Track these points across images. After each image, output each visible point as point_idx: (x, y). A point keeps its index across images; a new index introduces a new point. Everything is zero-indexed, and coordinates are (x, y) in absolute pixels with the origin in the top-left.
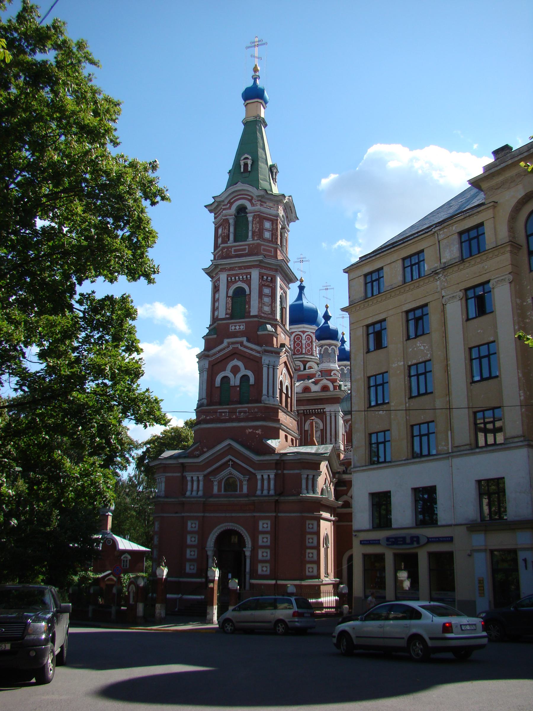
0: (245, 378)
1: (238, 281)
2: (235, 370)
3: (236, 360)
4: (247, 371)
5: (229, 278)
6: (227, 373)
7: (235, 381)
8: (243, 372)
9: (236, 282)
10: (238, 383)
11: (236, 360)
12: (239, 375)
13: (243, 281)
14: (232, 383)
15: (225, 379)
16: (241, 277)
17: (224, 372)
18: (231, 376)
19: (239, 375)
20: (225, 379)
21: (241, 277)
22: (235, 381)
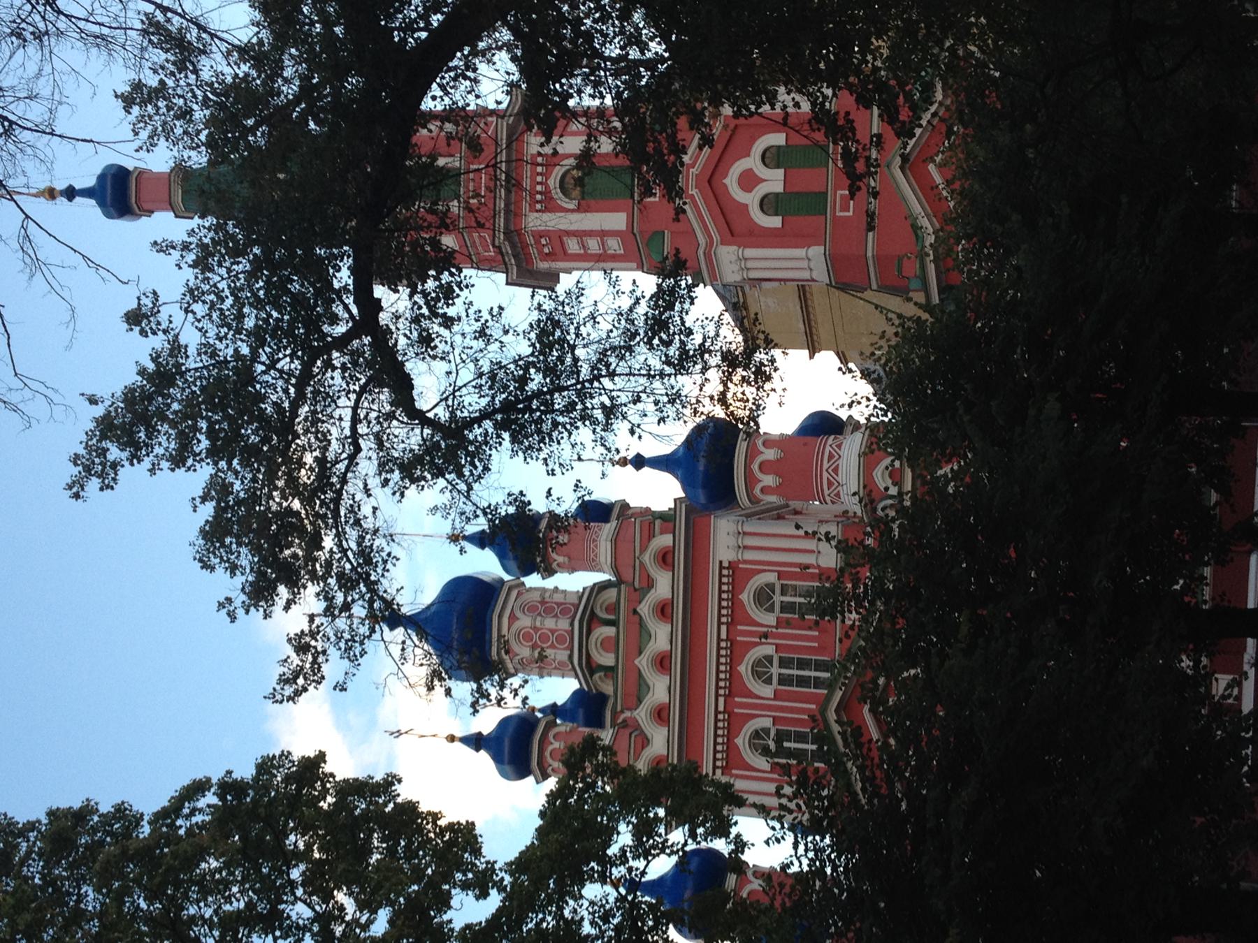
0: (772, 158)
1: (547, 186)
2: (749, 180)
3: (727, 181)
4: (752, 154)
5: (538, 206)
6: (751, 200)
7: (774, 180)
8: (752, 162)
9: (547, 193)
10: (780, 173)
11: (727, 181)
12: (762, 171)
13: (546, 175)
14: (778, 188)
15: (768, 204)
16: (539, 179)
17: (750, 208)
18: (761, 190)
19: (762, 171)
20: (768, 204)
21: (539, 179)
22: (774, 180)
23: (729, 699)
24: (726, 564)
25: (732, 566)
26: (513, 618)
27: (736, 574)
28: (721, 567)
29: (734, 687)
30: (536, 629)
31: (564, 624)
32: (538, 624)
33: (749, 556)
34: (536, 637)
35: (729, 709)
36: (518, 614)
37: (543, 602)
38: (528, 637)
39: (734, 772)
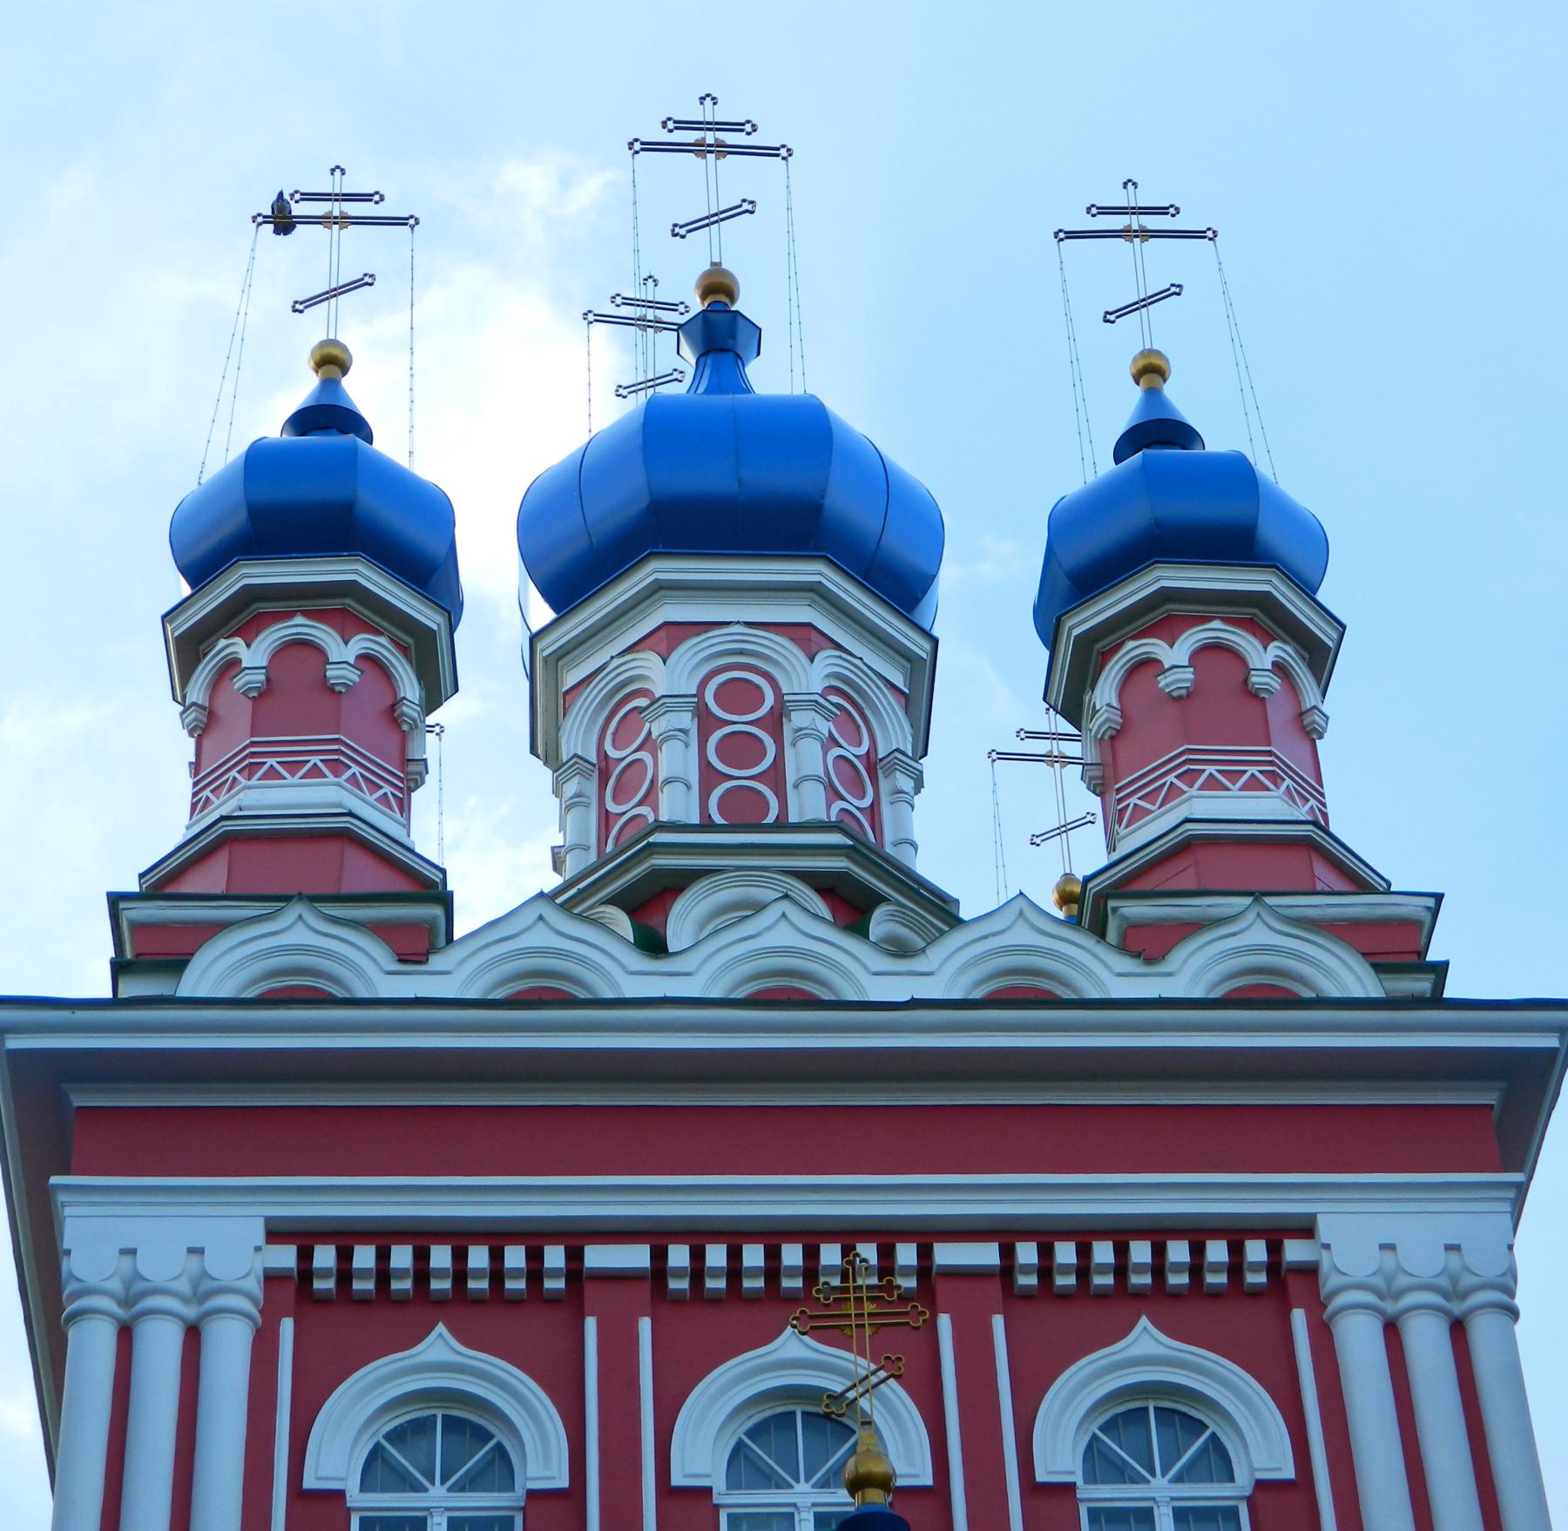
23: (645, 1290)
24: (1295, 1251)
25: (1295, 1285)
26: (806, 637)
27: (1261, 1302)
28: (1276, 1233)
29: (707, 1312)
30: (775, 722)
31: (808, 803)
32: (799, 719)
33: (1359, 1342)
34: (741, 722)
35: (591, 1292)
36: (826, 658)
37: (871, 762)
38: (739, 695)
39: (287, 1326)
